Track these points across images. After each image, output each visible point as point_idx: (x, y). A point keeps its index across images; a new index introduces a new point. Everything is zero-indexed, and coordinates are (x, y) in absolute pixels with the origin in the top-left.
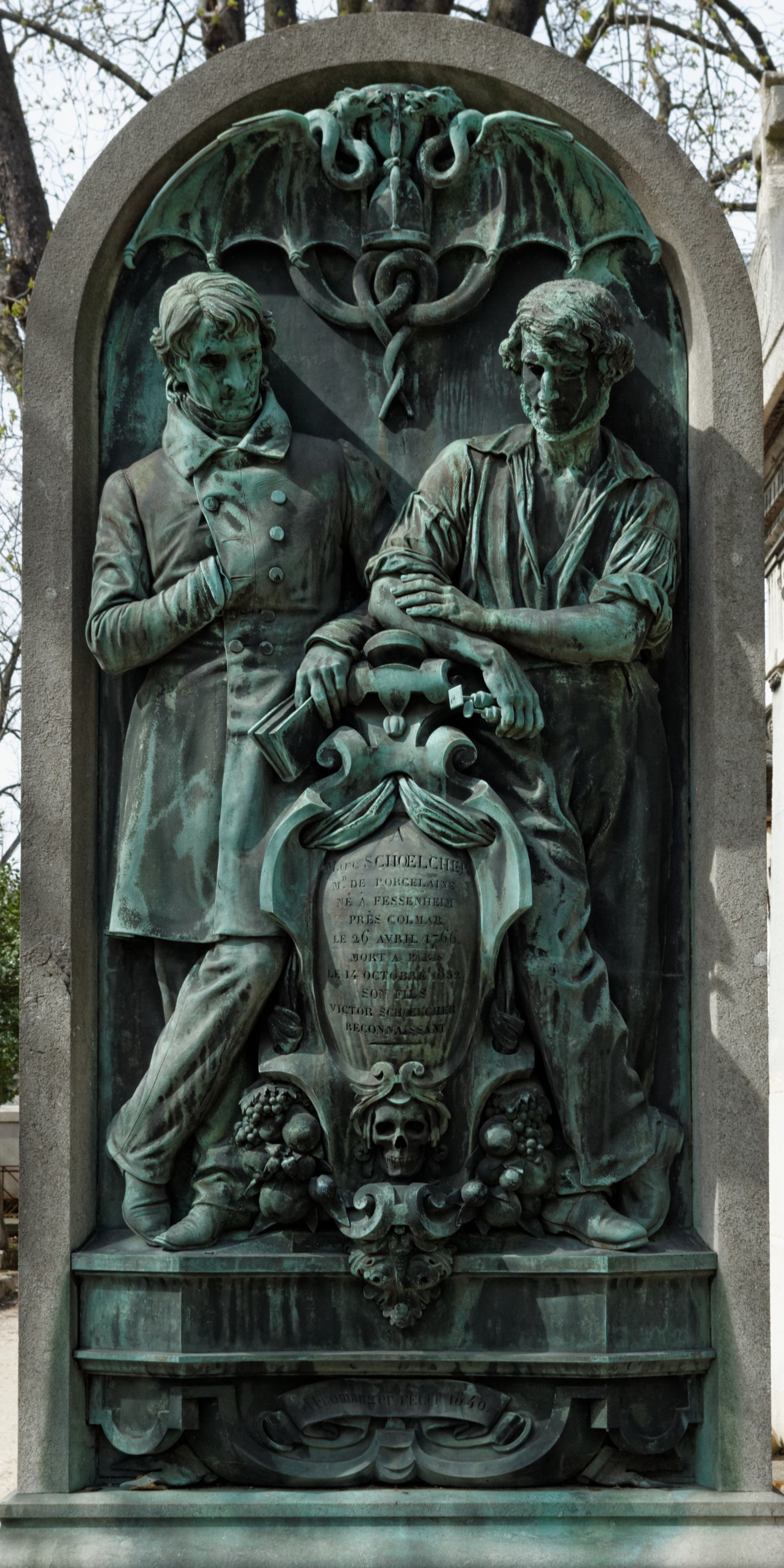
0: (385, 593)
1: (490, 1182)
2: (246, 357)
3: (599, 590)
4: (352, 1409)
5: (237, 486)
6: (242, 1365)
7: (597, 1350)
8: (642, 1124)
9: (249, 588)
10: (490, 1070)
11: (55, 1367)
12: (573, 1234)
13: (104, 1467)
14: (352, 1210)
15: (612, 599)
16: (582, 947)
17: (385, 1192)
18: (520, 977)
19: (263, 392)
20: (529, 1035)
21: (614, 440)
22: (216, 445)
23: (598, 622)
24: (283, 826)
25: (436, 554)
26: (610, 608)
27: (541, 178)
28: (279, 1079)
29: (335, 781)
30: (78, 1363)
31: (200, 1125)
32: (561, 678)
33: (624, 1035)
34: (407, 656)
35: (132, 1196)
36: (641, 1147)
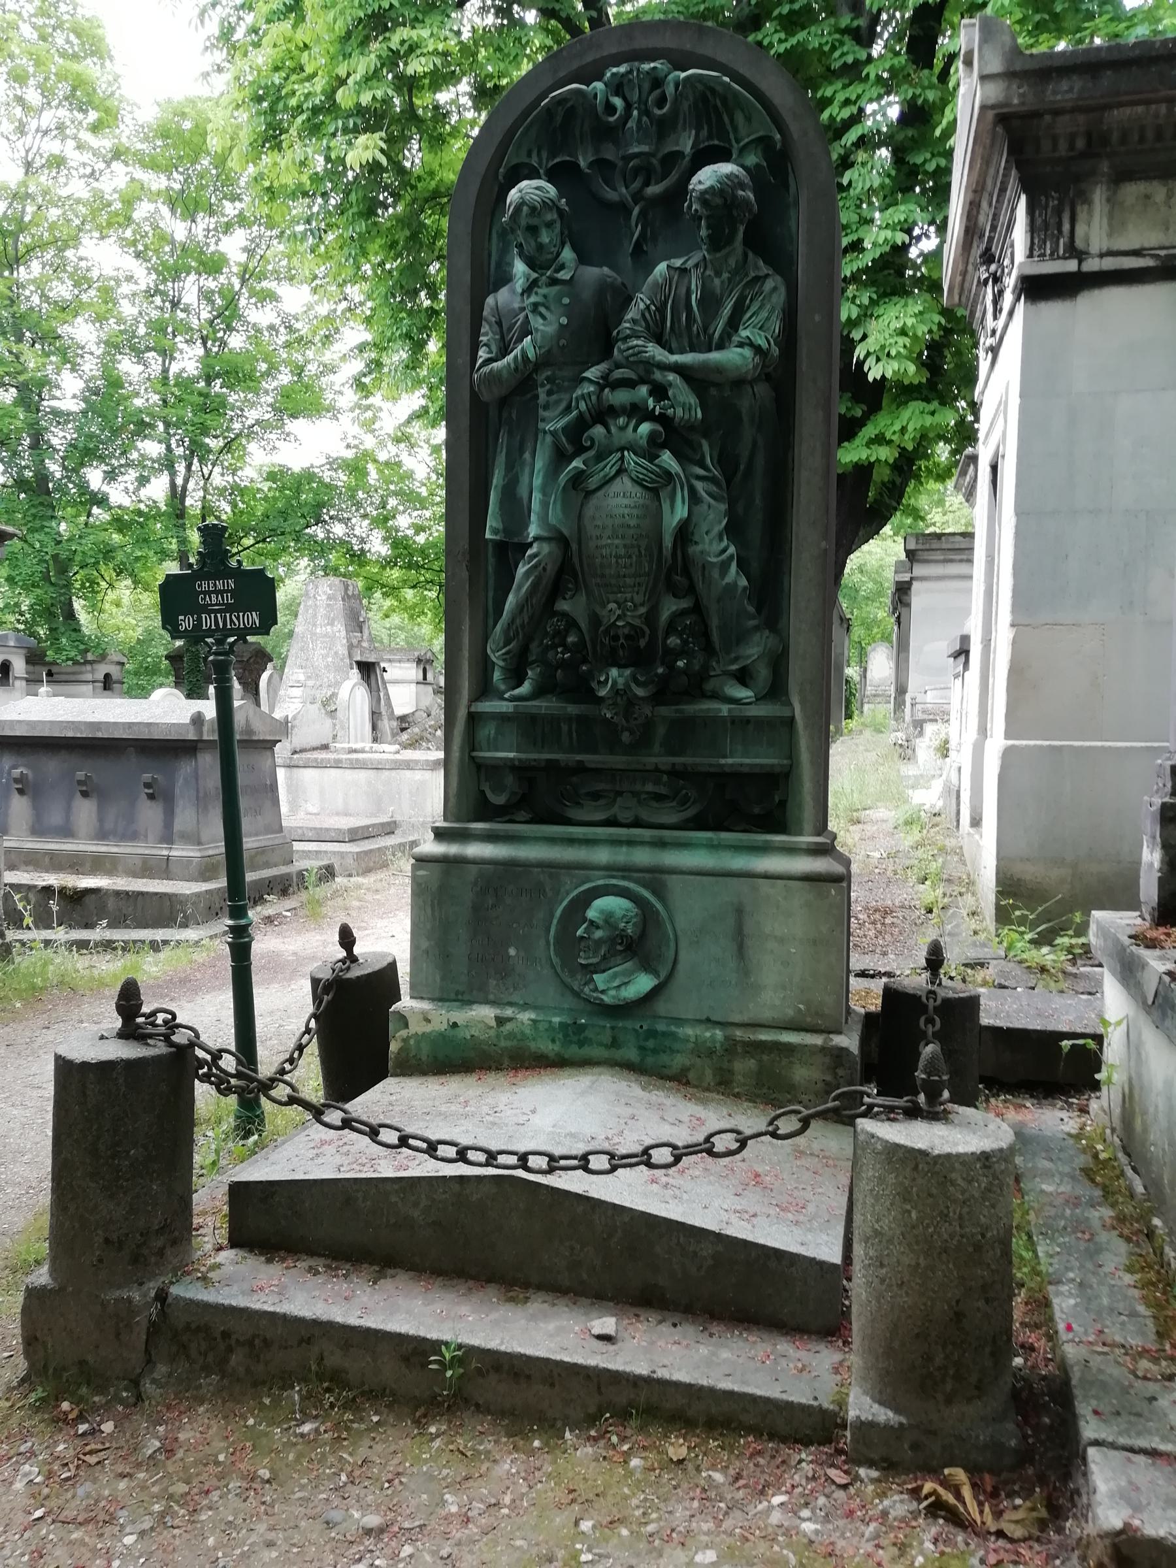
0: (621, 351)
1: (671, 667)
2: (549, 225)
3: (735, 339)
4: (601, 786)
5: (545, 296)
6: (548, 761)
7: (725, 757)
8: (756, 637)
9: (549, 351)
10: (670, 607)
11: (461, 760)
12: (717, 696)
13: (483, 810)
14: (599, 682)
15: (741, 345)
16: (721, 540)
17: (614, 672)
18: (685, 556)
19: (563, 244)
20: (691, 590)
21: (751, 255)
22: (535, 275)
23: (733, 357)
24: (563, 478)
25: (648, 327)
26: (739, 350)
27: (715, 106)
28: (564, 615)
29: (592, 453)
30: (473, 758)
31: (528, 640)
32: (713, 391)
33: (745, 588)
34: (630, 384)
35: (497, 675)
36: (753, 650)
